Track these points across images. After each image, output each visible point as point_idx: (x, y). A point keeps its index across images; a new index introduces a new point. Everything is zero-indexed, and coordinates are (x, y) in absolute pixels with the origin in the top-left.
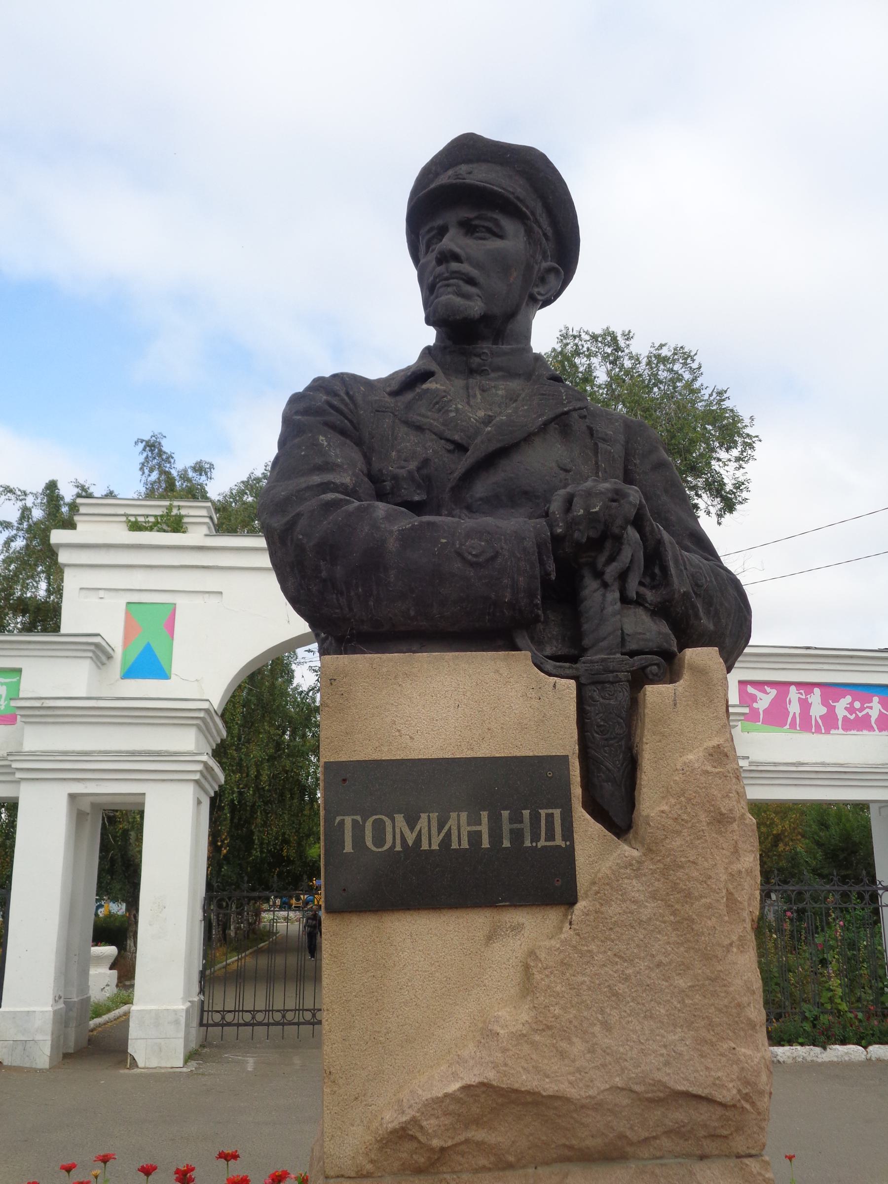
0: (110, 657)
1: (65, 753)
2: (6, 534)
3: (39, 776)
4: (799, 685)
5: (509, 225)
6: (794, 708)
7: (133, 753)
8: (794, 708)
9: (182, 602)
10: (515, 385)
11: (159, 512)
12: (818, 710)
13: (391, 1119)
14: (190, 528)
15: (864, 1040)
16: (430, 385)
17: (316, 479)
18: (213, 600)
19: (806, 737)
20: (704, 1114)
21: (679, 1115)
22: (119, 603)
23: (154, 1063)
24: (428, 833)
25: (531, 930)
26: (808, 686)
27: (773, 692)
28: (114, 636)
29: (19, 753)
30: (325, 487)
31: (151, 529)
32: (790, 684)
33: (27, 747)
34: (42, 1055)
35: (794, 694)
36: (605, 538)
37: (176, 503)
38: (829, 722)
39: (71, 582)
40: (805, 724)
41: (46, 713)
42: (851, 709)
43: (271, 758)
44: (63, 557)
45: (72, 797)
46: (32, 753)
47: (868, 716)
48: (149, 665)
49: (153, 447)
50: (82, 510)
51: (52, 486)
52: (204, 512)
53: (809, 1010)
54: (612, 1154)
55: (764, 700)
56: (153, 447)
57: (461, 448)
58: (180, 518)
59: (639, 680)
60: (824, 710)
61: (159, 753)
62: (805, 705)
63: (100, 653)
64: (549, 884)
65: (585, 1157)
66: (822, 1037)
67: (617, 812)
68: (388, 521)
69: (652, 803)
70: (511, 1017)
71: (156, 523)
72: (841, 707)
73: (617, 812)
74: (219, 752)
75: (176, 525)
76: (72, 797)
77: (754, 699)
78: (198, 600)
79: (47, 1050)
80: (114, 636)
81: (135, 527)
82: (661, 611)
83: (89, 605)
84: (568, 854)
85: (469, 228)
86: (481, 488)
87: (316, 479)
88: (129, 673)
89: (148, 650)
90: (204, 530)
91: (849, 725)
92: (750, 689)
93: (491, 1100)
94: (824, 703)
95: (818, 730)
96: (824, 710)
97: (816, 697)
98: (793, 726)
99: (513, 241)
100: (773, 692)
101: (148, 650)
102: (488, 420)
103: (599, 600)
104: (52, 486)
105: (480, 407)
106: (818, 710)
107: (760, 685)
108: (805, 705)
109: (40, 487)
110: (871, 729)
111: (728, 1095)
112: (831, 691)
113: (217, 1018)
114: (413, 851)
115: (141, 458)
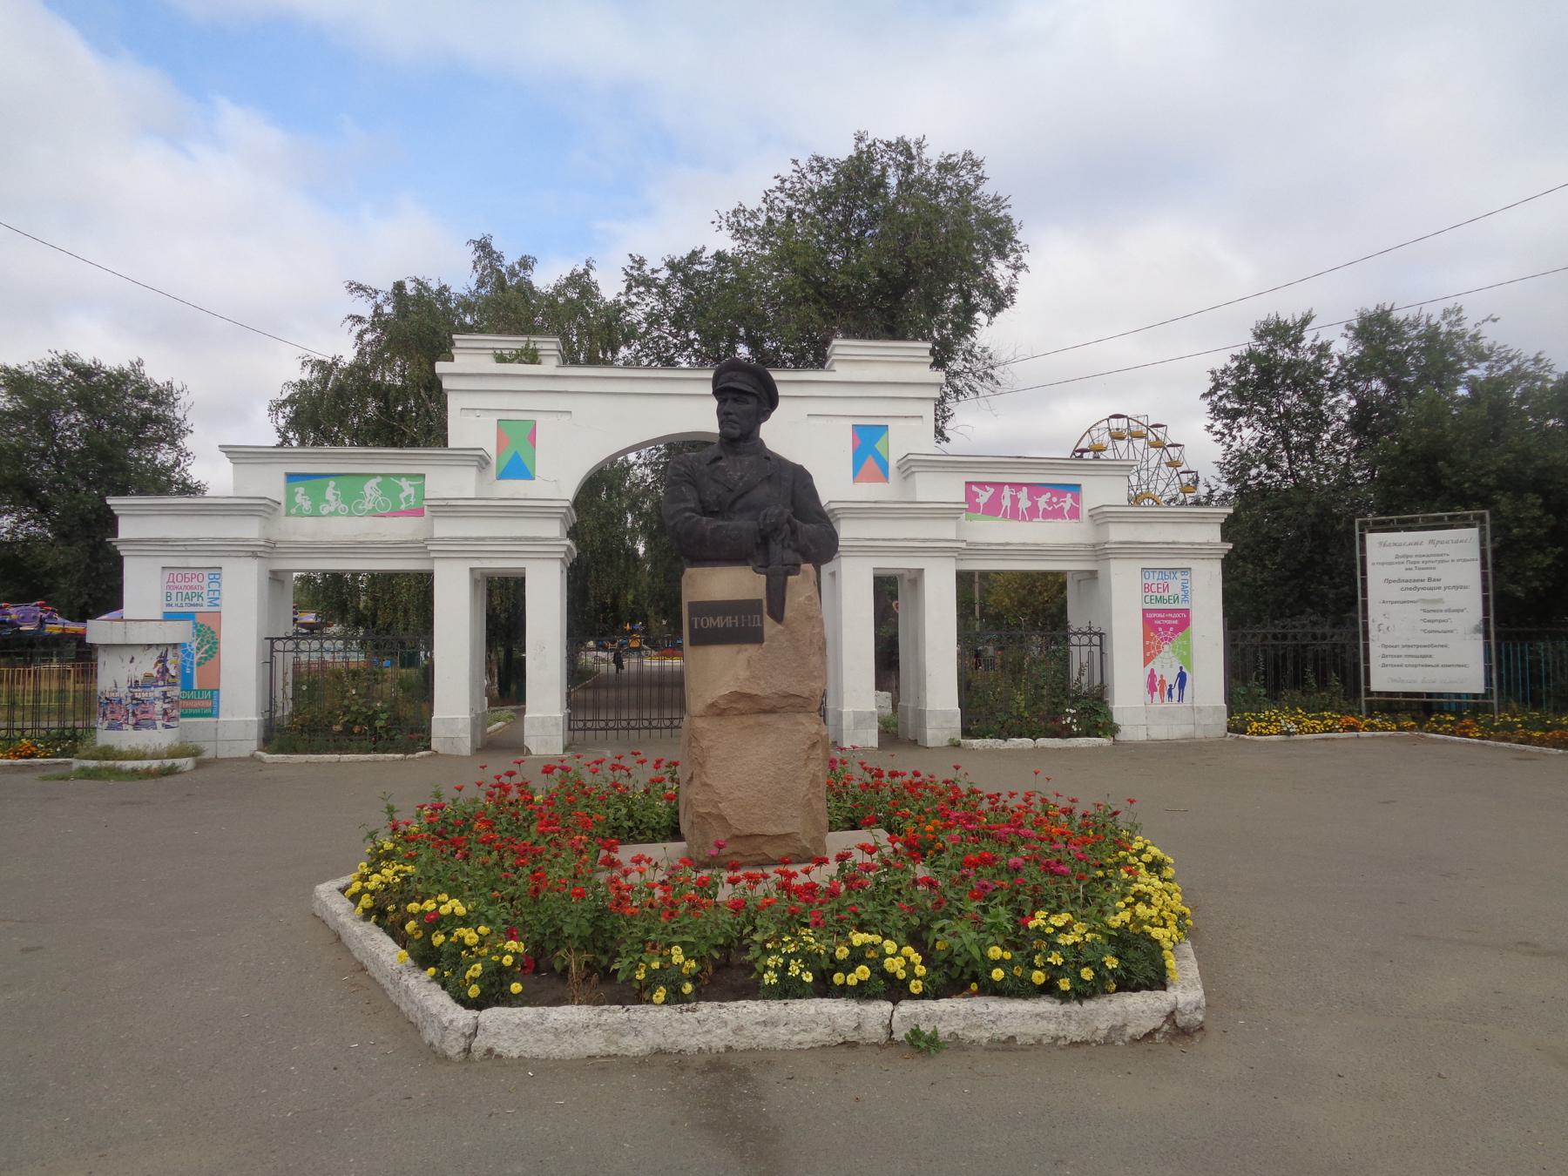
0: (488, 463)
1: (466, 539)
2: (358, 328)
3: (448, 556)
4: (1011, 485)
5: (750, 399)
6: (1006, 502)
7: (515, 539)
8: (1006, 502)
9: (541, 420)
10: (751, 458)
11: (519, 346)
12: (1024, 503)
13: (710, 701)
14: (544, 360)
15: (1033, 735)
16: (721, 464)
17: (682, 506)
18: (566, 417)
19: (1015, 523)
20: (799, 700)
21: (792, 701)
22: (494, 418)
23: (542, 752)
24: (719, 622)
25: (750, 650)
26: (1018, 486)
27: (991, 490)
28: (491, 449)
29: (432, 539)
30: (686, 510)
31: (511, 361)
32: (1003, 484)
33: (436, 535)
34: (465, 748)
35: (1007, 491)
36: (776, 529)
37: (533, 339)
38: (1033, 512)
39: (454, 404)
40: (1014, 514)
41: (449, 509)
42: (1049, 503)
43: (601, 526)
44: (446, 384)
45: (472, 570)
46: (442, 539)
47: (1062, 508)
48: (518, 469)
49: (484, 247)
50: (458, 344)
51: (399, 286)
52: (554, 346)
53: (1001, 716)
54: (772, 711)
55: (984, 497)
56: (484, 247)
57: (731, 490)
58: (535, 350)
59: (788, 573)
60: (1029, 504)
61: (534, 539)
62: (1015, 500)
63: (482, 462)
64: (755, 637)
65: (765, 712)
66: (1005, 732)
67: (778, 616)
68: (708, 523)
69: (788, 613)
70: (744, 674)
71: (517, 356)
72: (1042, 502)
73: (778, 616)
74: (573, 533)
75: (532, 357)
76: (472, 570)
77: (977, 495)
78: (553, 418)
79: (469, 743)
80: (491, 449)
81: (501, 359)
82: (796, 550)
83: (469, 423)
84: (761, 629)
85: (735, 400)
86: (739, 505)
87: (682, 506)
88: (502, 476)
89: (516, 456)
90: (554, 362)
91: (1048, 515)
92: (974, 488)
93: (739, 696)
94: (1030, 498)
95: (1024, 519)
96: (1029, 504)
97: (1023, 494)
98: (1005, 516)
99: (751, 405)
100: (991, 490)
101: (516, 456)
102: (741, 478)
103: (775, 548)
104: (399, 286)
105: (736, 470)
106: (1024, 503)
107: (981, 485)
108: (1015, 500)
109: (389, 288)
110: (1063, 517)
111: (806, 695)
112: (1035, 489)
113: (581, 724)
114: (715, 628)
115: (474, 257)
